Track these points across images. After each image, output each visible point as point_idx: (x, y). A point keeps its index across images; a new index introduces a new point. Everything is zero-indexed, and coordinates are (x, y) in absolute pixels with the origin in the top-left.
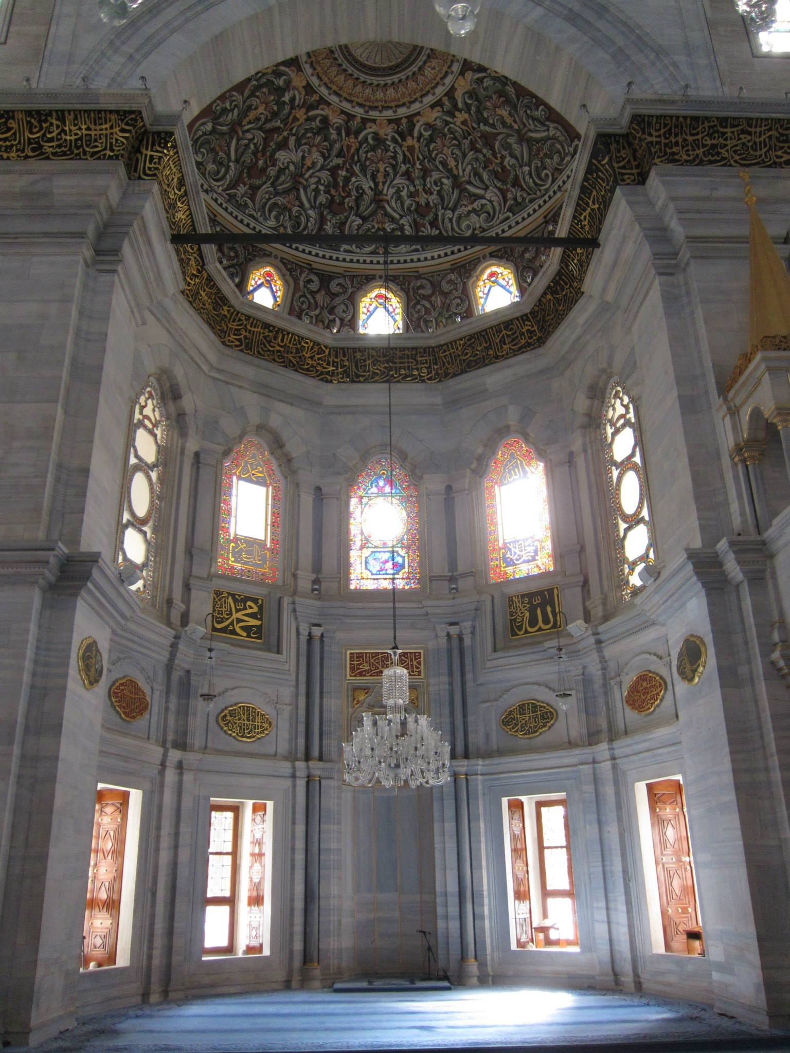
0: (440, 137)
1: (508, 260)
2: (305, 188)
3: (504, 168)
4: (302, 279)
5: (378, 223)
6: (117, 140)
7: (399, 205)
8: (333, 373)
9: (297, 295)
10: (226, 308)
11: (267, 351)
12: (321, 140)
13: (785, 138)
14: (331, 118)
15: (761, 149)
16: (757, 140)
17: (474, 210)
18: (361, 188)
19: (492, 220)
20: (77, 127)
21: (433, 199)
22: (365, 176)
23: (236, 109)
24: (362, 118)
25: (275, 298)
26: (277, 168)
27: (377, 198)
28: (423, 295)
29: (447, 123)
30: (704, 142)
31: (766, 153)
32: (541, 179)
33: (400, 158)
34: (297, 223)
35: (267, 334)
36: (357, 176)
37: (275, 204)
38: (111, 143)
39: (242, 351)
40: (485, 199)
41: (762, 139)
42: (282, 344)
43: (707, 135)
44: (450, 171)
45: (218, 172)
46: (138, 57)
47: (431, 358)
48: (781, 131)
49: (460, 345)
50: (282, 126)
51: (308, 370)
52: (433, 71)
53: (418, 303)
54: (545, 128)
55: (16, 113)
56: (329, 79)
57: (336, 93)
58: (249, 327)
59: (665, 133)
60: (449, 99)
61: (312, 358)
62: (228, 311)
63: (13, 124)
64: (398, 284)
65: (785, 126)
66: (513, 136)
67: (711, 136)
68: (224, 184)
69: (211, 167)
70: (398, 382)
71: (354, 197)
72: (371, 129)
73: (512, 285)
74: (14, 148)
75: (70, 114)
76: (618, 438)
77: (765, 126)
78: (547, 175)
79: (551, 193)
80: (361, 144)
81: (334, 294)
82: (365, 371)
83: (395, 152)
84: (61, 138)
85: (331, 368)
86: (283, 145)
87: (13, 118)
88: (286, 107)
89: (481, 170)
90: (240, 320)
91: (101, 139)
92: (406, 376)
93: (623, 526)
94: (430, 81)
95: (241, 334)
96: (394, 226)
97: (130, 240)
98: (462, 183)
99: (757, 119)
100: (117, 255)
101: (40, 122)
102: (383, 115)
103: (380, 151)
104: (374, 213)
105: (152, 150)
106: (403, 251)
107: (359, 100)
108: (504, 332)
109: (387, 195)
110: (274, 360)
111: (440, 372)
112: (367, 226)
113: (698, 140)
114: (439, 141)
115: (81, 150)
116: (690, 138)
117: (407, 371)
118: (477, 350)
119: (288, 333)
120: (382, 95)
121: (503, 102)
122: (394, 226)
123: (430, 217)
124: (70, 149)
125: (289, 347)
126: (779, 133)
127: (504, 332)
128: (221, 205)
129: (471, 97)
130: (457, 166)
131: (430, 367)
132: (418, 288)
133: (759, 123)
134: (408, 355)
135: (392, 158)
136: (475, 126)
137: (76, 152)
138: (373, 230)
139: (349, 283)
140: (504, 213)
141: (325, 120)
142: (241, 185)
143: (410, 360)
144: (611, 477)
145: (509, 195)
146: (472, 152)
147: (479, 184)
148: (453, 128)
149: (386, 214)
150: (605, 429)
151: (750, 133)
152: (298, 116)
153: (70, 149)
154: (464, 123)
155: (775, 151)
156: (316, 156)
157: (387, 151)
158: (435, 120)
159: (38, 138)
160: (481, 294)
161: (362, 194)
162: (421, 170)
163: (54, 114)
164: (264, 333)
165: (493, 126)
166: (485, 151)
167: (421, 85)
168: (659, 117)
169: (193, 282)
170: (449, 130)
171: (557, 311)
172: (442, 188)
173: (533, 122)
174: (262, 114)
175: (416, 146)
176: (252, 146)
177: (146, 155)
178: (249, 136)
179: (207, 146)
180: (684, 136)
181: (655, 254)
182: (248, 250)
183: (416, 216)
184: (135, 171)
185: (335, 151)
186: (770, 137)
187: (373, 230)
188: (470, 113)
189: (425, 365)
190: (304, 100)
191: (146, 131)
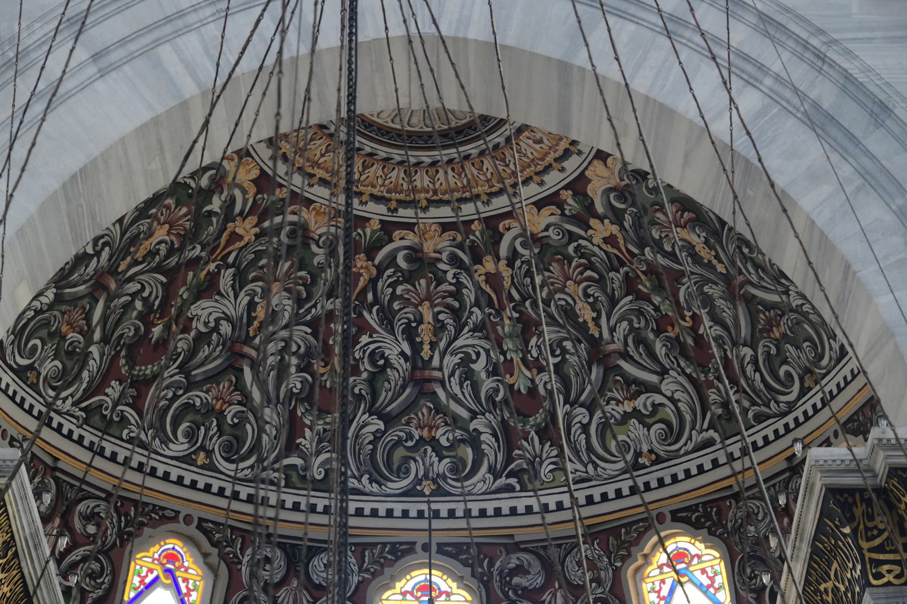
0: (558, 261)
1: (710, 534)
2: (254, 365)
3: (699, 340)
4: (246, 559)
5: (420, 427)
7: (468, 389)
12: (291, 267)
14: (312, 226)
17: (636, 413)
18: (382, 356)
19: (676, 441)
21: (547, 381)
22: (392, 332)
23: (107, 249)
24: (381, 221)
26: (193, 333)
27: (418, 374)
28: (524, 589)
29: (572, 237)
33: (469, 295)
34: (236, 437)
36: (373, 331)
37: (188, 407)
40: (659, 392)
44: (582, 327)
50: (204, 254)
52: (537, 147)
54: (780, 289)
57: (323, 182)
60: (575, 195)
64: (465, 563)
66: (716, 284)
68: (77, 390)
71: (365, 375)
72: (402, 240)
78: (788, 375)
79: (799, 413)
80: (381, 270)
81: (319, 587)
83: (459, 285)
88: (214, 220)
89: (651, 336)
94: (532, 161)
96: (458, 433)
98: (609, 355)
102: (428, 215)
103: (423, 282)
104: (411, 407)
106: (475, 491)
107: (375, 191)
109: (440, 369)
114: (555, 267)
120: (427, 180)
121: (690, 220)
122: (458, 433)
123: (540, 417)
128: (69, 436)
129: (621, 197)
130: (596, 320)
132: (514, 572)
135: (451, 294)
136: (636, 251)
138: (410, 444)
139: (353, 560)
141: (301, 232)
142: (113, 383)
145: (713, 396)
146: (630, 298)
147: (646, 361)
148: (585, 247)
149: (439, 409)
152: (239, 231)
154: (610, 240)
156: (281, 300)
157: (440, 282)
158: (547, 229)
161: (383, 369)
162: (518, 320)
165: (672, 256)
166: (657, 300)
167: (512, 166)
170: (577, 249)
172: (564, 361)
173: (757, 272)
174: (159, 243)
175: (506, 273)
176: (139, 305)
178: (133, 287)
179: (44, 333)
182: (127, 515)
183: (507, 415)
187: (410, 444)
188: (622, 227)
190: (255, 201)
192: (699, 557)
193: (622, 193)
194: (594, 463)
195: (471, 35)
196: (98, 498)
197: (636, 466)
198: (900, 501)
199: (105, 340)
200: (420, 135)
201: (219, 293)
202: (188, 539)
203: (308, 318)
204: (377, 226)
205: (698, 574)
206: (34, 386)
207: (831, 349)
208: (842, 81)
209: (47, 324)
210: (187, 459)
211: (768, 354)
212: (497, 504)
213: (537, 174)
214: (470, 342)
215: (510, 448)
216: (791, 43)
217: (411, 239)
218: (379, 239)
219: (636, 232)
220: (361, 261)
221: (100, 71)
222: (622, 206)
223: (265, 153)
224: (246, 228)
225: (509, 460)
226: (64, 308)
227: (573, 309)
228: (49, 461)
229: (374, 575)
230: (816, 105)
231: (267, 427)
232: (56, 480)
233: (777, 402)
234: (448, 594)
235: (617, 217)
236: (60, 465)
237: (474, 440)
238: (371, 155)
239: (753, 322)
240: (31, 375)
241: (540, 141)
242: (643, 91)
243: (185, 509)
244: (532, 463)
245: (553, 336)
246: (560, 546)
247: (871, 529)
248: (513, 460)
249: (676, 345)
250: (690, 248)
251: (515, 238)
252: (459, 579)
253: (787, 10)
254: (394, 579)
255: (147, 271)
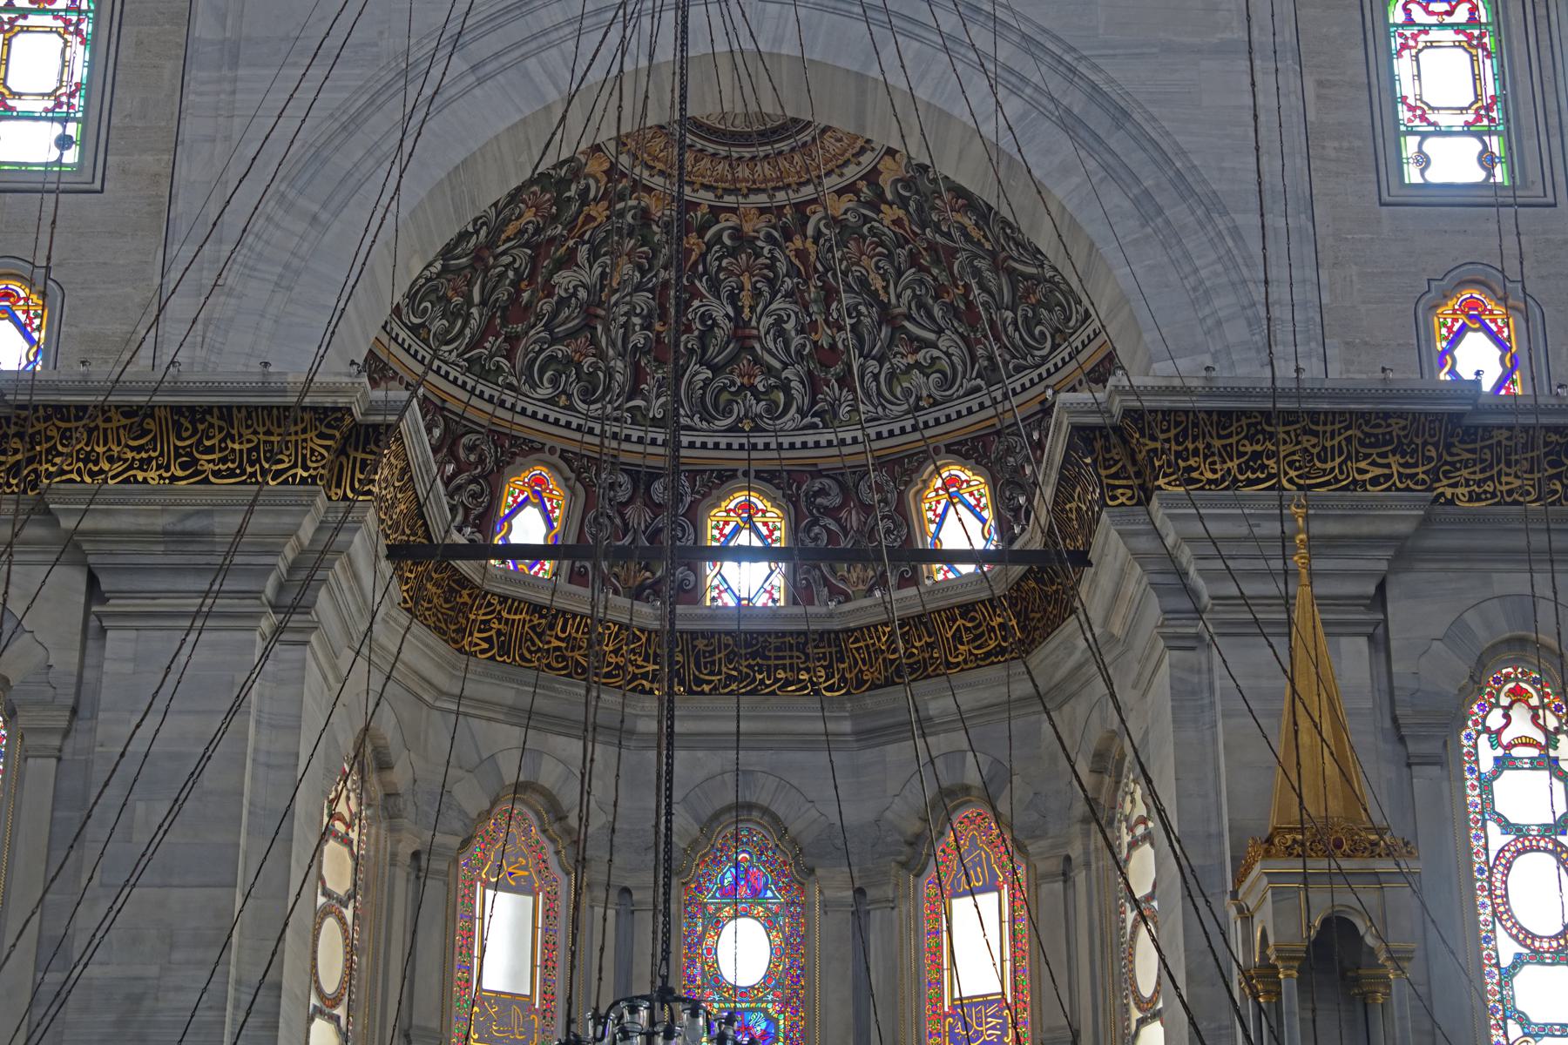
0: (854, 239)
1: (977, 463)
5: (741, 375)
6: (313, 451)
8: (655, 676)
9: (592, 514)
10: (465, 593)
11: (536, 652)
13: (1373, 440)
15: (1333, 460)
16: (1328, 444)
17: (917, 365)
18: (711, 317)
19: (950, 388)
20: (251, 430)
21: (845, 338)
25: (549, 522)
28: (826, 508)
29: (866, 220)
30: (1242, 449)
31: (1340, 465)
32: (1032, 336)
33: (782, 267)
35: (536, 622)
36: (702, 297)
38: (304, 456)
39: (492, 658)
40: (937, 348)
41: (1335, 442)
42: (563, 636)
43: (1246, 437)
44: (875, 294)
45: (448, 331)
46: (324, 216)
47: (834, 650)
48: (1367, 429)
49: (884, 634)
50: (565, 232)
51: (608, 675)
52: (838, 144)
53: (815, 522)
54: (1037, 263)
55: (157, 409)
56: (649, 155)
57: (661, 173)
58: (505, 614)
59: (1177, 436)
61: (616, 652)
62: (470, 595)
63: (150, 424)
64: (778, 487)
65: (1373, 422)
67: (1251, 439)
68: (461, 344)
69: (438, 324)
70: (773, 693)
71: (696, 333)
72: (727, 222)
73: (986, 507)
74: (154, 463)
75: (239, 412)
76: (1136, 854)
77: (1340, 422)
78: (1042, 333)
79: (1050, 365)
80: (709, 246)
81: (659, 505)
82: (712, 673)
83: (773, 259)
84: (226, 447)
85: (651, 667)
86: (569, 261)
87: (152, 416)
89: (930, 301)
90: (490, 604)
91: (287, 449)
92: (788, 683)
93: (1136, 1015)
95: (491, 629)
96: (772, 381)
97: (330, 591)
99: (1326, 413)
100: (309, 613)
101: (193, 423)
103: (743, 256)
104: (733, 359)
105: (364, 451)
107: (705, 181)
108: (960, 622)
109: (758, 329)
110: (549, 666)
111: (847, 675)
112: (722, 381)
113: (1231, 445)
114: (852, 244)
115: (257, 466)
116: (1217, 443)
117: (789, 674)
118: (914, 646)
119: (575, 616)
120: (747, 172)
121: (963, 206)
122: (772, 381)
123: (839, 367)
124: (240, 466)
125: (575, 639)
126: (1362, 431)
127: (960, 622)
128: (455, 382)
129: (907, 187)
130: (886, 288)
131: (830, 666)
133: (1330, 418)
134: (791, 645)
135: (766, 266)
136: (918, 231)
137: (249, 470)
138: (733, 389)
140: (971, 379)
141: (644, 215)
143: (796, 654)
144: (1124, 921)
145: (980, 351)
146: (913, 270)
147: (926, 322)
148: (877, 228)
149: (757, 361)
150: (1119, 830)
151: (1316, 434)
153: (240, 466)
154: (897, 222)
155: (1357, 461)
156: (627, 268)
158: (845, 213)
159: (190, 446)
160: (930, 515)
161: (711, 327)
162: (822, 288)
163: (216, 411)
164: (531, 621)
165: (948, 235)
166: (935, 271)
168: (1166, 413)
169: (413, 576)
170: (870, 229)
171: (1045, 610)
172: (859, 321)
174: (528, 223)
175: (812, 249)
176: (511, 274)
177: (355, 459)
178: (506, 259)
179: (433, 297)
180: (1208, 439)
181: (1165, 612)
182: (502, 446)
184: (338, 486)
185: (661, 260)
186: (1348, 440)
187: (733, 389)
188: (907, 211)
189: (822, 662)
191: (356, 425)
192: (968, 482)
193: (908, 183)
194: (883, 405)
195: (784, 51)
196: (478, 432)
197: (917, 408)
198: (1132, 437)
199: (483, 303)
200: (741, 134)
201: (577, 265)
202: (552, 467)
203: (650, 285)
204: (706, 210)
205: (967, 496)
206: (425, 341)
207: (1077, 312)
208: (1089, 90)
209: (435, 289)
210: (551, 401)
211: (1026, 317)
212: (804, 439)
213: (838, 167)
214: (782, 306)
215: (814, 393)
216: (1048, 59)
217: (734, 220)
218: (707, 221)
219: (919, 216)
220: (693, 238)
221: (478, 79)
222: (907, 194)
223: (612, 146)
224: (599, 211)
225: (814, 402)
226: (450, 276)
227: (867, 279)
228: (438, 403)
229: (704, 496)
230: (1068, 111)
231: (617, 375)
232: (445, 418)
233: (1033, 356)
234: (764, 512)
235: (903, 203)
236: (447, 405)
237: (785, 387)
238: (701, 151)
239: (1014, 289)
240: (423, 332)
241: (840, 140)
242: (925, 98)
243: (549, 442)
244: (832, 405)
245: (850, 301)
246: (854, 473)
247: (1108, 460)
248: (817, 403)
249: (951, 309)
250: (963, 229)
251: (820, 220)
252: (773, 501)
253: (1045, 31)
254: (720, 499)
255: (520, 246)
